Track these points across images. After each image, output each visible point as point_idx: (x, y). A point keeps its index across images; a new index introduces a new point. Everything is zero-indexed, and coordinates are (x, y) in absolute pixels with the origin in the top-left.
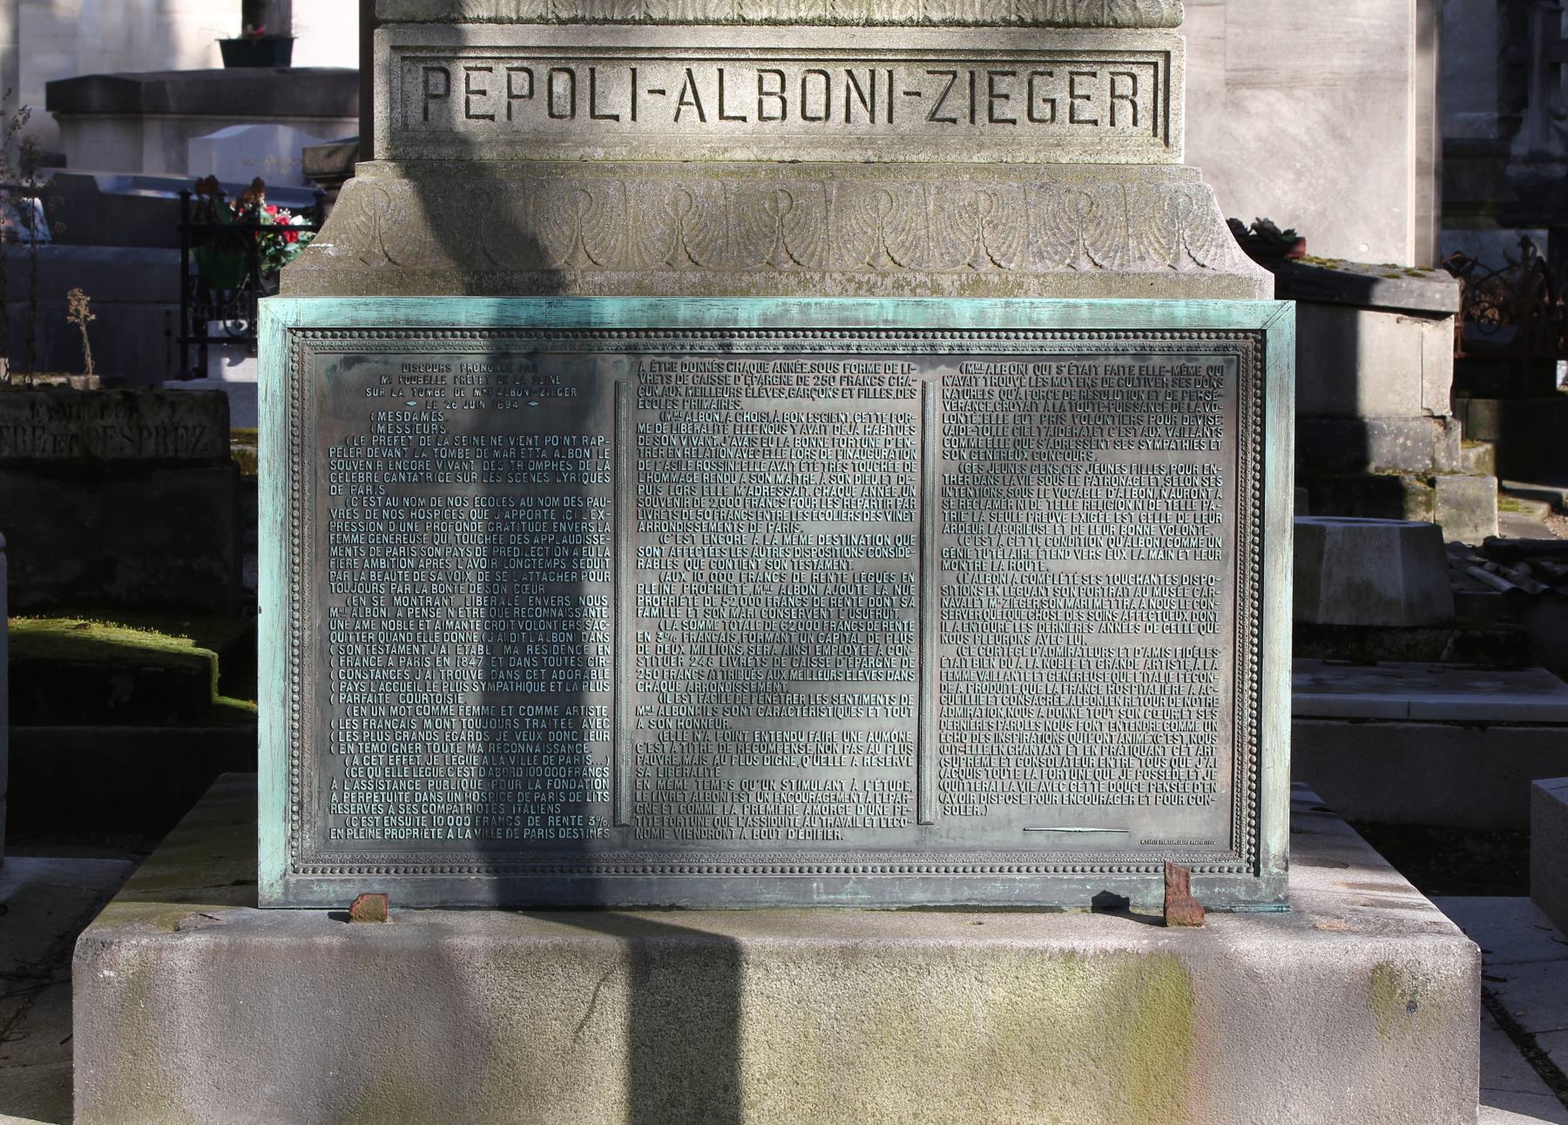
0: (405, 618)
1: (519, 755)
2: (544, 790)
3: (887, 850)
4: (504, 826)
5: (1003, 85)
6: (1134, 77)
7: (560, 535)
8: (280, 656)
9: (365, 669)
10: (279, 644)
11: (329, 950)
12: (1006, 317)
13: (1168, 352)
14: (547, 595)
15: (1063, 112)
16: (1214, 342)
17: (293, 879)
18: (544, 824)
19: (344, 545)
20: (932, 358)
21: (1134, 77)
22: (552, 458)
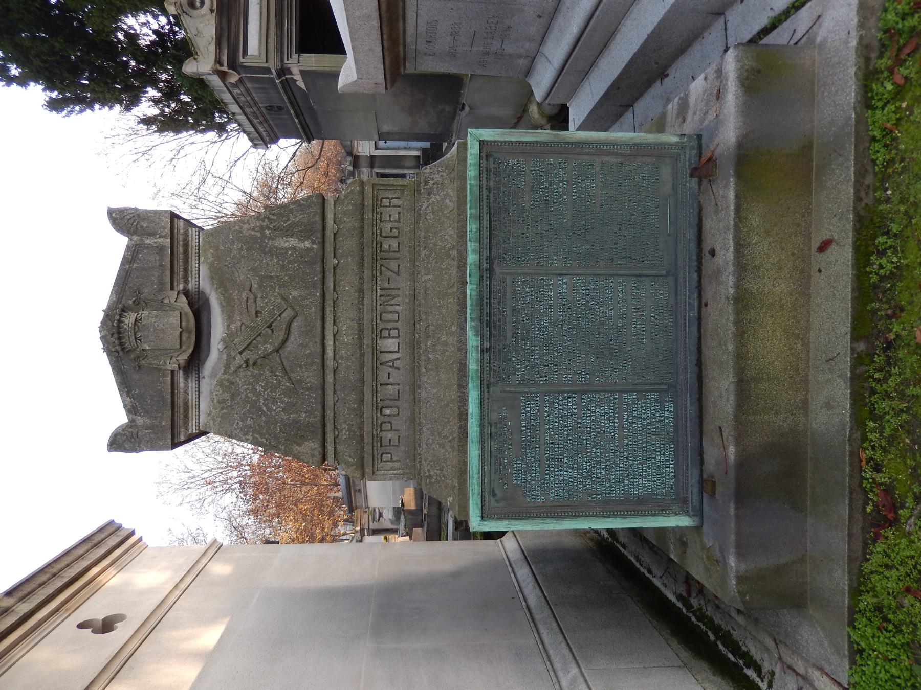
0: (591, 472)
1: (642, 428)
2: (655, 418)
3: (677, 288)
4: (668, 433)
5: (386, 247)
6: (382, 198)
7: (559, 413)
8: (607, 520)
9: (611, 486)
10: (603, 520)
11: (737, 509)
12: (476, 242)
13: (488, 179)
14: (582, 417)
15: (396, 225)
16: (485, 162)
17: (691, 513)
18: (668, 417)
19: (564, 495)
20: (491, 270)
21: (382, 198)
22: (530, 416)
